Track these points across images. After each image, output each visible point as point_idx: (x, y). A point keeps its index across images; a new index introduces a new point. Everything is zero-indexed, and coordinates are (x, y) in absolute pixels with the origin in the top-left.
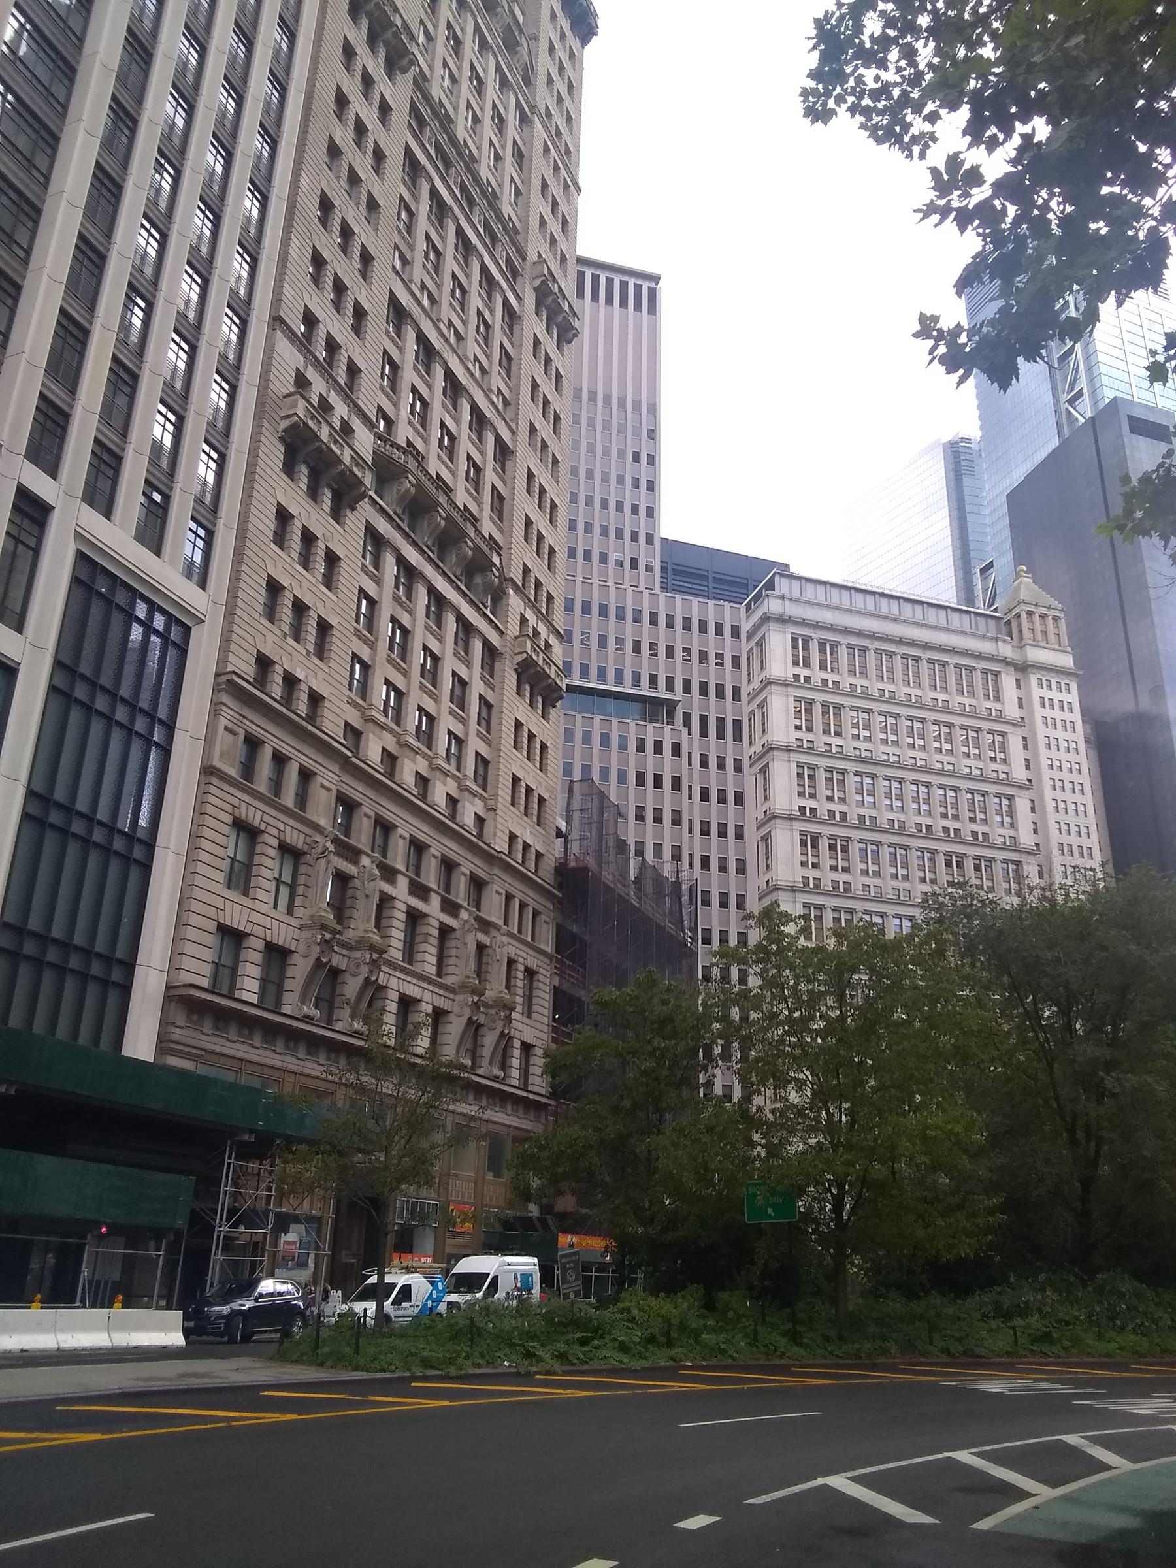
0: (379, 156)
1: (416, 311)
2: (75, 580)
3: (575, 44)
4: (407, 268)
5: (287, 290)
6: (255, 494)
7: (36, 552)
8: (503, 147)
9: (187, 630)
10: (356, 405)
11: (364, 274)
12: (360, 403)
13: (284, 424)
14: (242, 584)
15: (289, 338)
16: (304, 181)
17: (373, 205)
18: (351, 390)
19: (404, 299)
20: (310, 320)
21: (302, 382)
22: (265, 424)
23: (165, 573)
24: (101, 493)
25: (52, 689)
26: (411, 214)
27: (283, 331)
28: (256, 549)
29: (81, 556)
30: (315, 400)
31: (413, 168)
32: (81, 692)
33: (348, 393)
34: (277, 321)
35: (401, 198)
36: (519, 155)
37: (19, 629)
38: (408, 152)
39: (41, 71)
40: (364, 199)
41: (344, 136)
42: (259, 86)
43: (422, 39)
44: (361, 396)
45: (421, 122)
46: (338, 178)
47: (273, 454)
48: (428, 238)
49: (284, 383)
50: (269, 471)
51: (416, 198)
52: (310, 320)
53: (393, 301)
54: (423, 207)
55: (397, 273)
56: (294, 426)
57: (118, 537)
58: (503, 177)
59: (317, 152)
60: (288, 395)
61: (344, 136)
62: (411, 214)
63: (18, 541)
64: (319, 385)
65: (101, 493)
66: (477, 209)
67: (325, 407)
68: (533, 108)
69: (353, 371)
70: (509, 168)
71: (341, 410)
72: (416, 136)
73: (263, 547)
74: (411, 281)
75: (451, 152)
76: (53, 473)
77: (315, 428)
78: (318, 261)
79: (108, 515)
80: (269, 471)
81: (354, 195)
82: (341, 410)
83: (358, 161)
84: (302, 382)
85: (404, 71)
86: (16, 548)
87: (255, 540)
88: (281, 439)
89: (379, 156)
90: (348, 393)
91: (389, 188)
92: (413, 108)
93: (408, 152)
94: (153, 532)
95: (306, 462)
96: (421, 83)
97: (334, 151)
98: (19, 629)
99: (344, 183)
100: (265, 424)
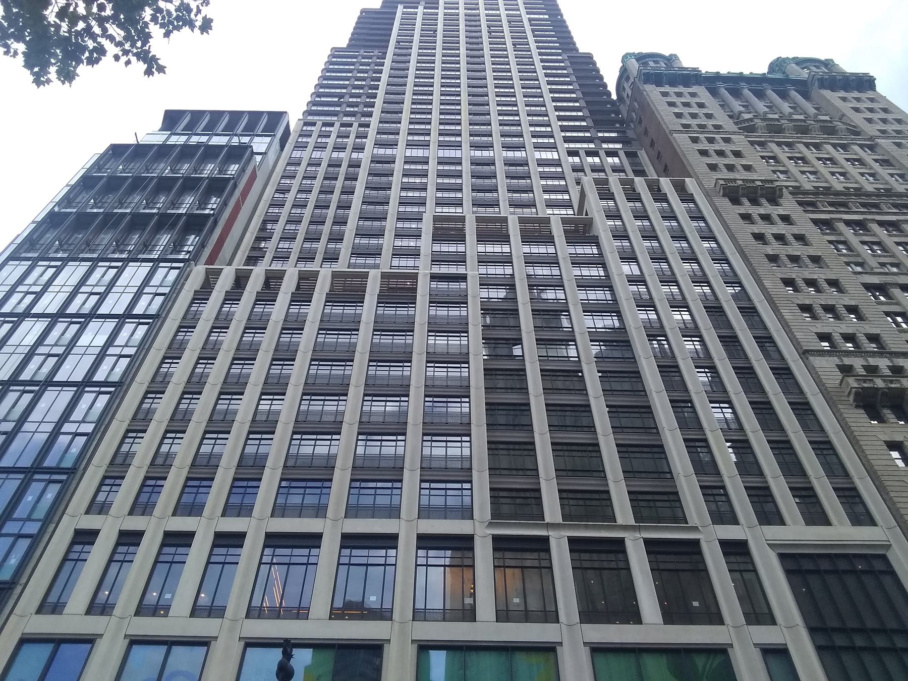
0: (800, 238)
1: (889, 279)
2: (788, 572)
3: (870, 94)
4: (865, 266)
5: (799, 335)
6: (864, 447)
7: (755, 571)
8: (871, 168)
9: (884, 558)
10: (891, 353)
11: (841, 290)
12: (893, 350)
13: (851, 398)
14: (899, 505)
15: (819, 356)
16: (767, 284)
17: (816, 260)
18: (883, 348)
19: (875, 280)
20: (823, 337)
21: (846, 370)
22: (840, 406)
23: (841, 532)
24: (768, 513)
25: (819, 649)
26: (844, 243)
27: (812, 355)
28: (892, 478)
29: (782, 557)
30: (862, 372)
31: (825, 225)
32: (840, 640)
33: (883, 351)
34: (805, 354)
35: (830, 242)
36: (885, 163)
37: (774, 622)
38: (816, 222)
39: (617, 354)
40: (808, 261)
41: (774, 247)
42: (713, 270)
43: (782, 176)
44: (891, 346)
45: (812, 204)
46: (785, 266)
47: (859, 419)
48: (863, 243)
49: (833, 377)
50: (863, 429)
51: (840, 234)
52: (823, 337)
53: (868, 287)
54: (848, 233)
55: (860, 273)
56: (857, 394)
57: (796, 531)
58: (883, 179)
59: (764, 267)
60: (842, 381)
61: (774, 247)
62: (844, 243)
63: (741, 571)
64: (858, 363)
65: (768, 513)
66: (883, 206)
67: (872, 370)
68: (871, 138)
69: (874, 338)
70: (883, 172)
71: (883, 363)
72: (813, 212)
73: (896, 473)
74: (872, 269)
75: (842, 199)
76: (736, 522)
77: (871, 385)
78: (806, 308)
79: (782, 523)
80: (863, 429)
81: (802, 265)
82: (883, 363)
83: (790, 250)
84: (846, 370)
85: (781, 196)
86: (742, 576)
87: (885, 473)
88: (857, 407)
89: (800, 238)
90: (883, 351)
91: (819, 242)
92: (800, 203)
93: (816, 222)
94: (815, 514)
95: (884, 407)
96: (796, 191)
97: (773, 259)
98: (774, 622)
99: (790, 265)
100: (840, 406)
